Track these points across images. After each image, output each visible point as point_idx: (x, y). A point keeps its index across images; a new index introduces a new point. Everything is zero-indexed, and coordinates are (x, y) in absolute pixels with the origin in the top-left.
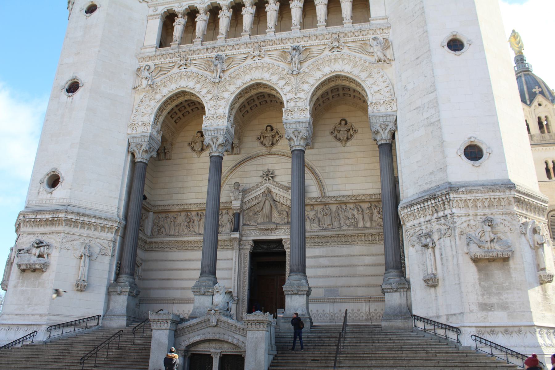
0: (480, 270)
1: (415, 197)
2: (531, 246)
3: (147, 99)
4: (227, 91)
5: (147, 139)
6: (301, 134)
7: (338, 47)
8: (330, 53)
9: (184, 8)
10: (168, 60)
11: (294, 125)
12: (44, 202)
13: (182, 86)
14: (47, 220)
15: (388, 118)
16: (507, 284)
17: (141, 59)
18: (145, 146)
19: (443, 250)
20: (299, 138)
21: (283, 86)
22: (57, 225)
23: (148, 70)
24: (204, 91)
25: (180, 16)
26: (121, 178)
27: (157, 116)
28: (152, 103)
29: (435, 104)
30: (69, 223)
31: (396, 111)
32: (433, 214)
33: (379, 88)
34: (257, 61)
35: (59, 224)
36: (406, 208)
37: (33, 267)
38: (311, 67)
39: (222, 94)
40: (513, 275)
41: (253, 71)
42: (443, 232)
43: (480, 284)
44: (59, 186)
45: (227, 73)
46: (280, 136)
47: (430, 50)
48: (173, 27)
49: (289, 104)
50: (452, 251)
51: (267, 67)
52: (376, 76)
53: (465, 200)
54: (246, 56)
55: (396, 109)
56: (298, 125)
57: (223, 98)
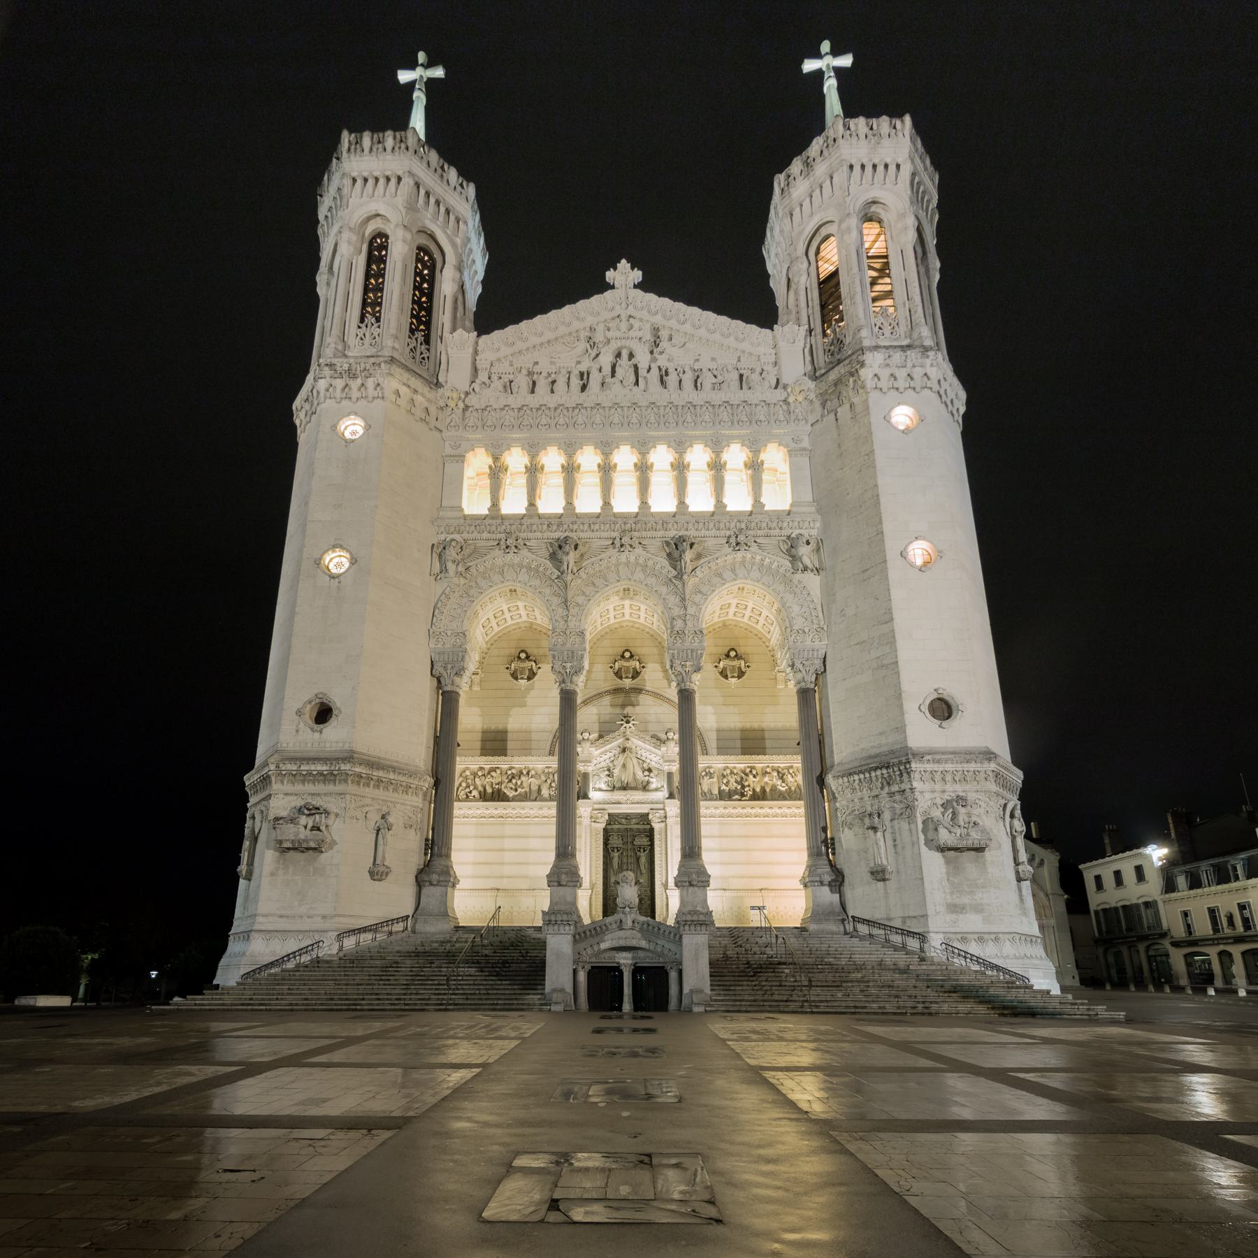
0: (948, 862)
1: (857, 764)
12: (309, 745)
14: (321, 773)
16: (982, 881)
19: (897, 835)
22: (337, 781)
30: (357, 779)
32: (882, 788)
35: (340, 781)
36: (842, 777)
37: (305, 845)
40: (989, 870)
42: (898, 812)
43: (948, 879)
44: (333, 722)
50: (911, 836)
53: (931, 772)
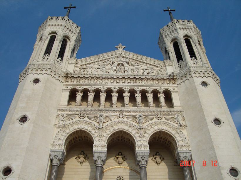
4: (106, 133)
5: (61, 153)
6: (145, 159)
8: (157, 120)
9: (82, 89)
10: (74, 112)
11: (142, 154)
13: (81, 127)
15: (187, 153)
18: (60, 157)
20: (144, 160)
21: (135, 133)
23: (63, 116)
25: (80, 92)
26: (45, 173)
28: (64, 134)
29: (212, 148)
31: (191, 150)
33: (182, 139)
38: (149, 126)
39: (103, 134)
41: (119, 125)
46: (126, 158)
47: (207, 124)
48: (76, 97)
49: (138, 143)
51: (126, 123)
52: (179, 133)
54: (115, 116)
56: (144, 154)
57: (104, 136)
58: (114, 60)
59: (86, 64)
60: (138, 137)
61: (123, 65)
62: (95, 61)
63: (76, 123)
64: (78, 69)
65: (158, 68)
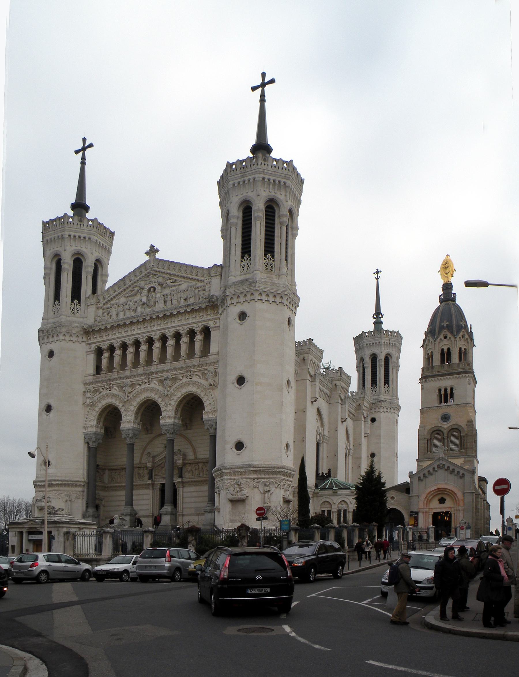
2: (261, 493)
3: (92, 410)
7: (190, 375)
11: (166, 426)
17: (85, 384)
21: (161, 402)
23: (89, 392)
24: (121, 405)
25: (105, 351)
27: (99, 419)
31: (217, 417)
33: (210, 402)
34: (147, 386)
39: (129, 407)
45: (132, 394)
52: (209, 394)
54: (141, 382)
55: (216, 416)
58: (142, 284)
59: (109, 301)
60: (164, 406)
61: (155, 289)
62: (119, 291)
63: (103, 398)
64: (100, 311)
65: (200, 284)
